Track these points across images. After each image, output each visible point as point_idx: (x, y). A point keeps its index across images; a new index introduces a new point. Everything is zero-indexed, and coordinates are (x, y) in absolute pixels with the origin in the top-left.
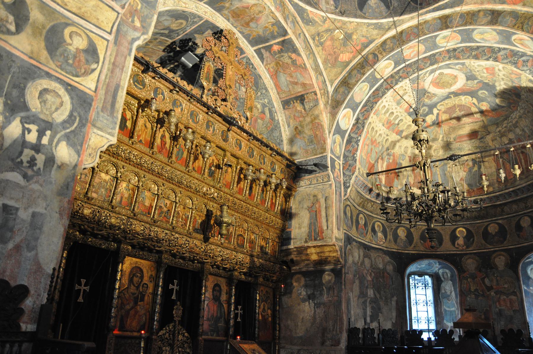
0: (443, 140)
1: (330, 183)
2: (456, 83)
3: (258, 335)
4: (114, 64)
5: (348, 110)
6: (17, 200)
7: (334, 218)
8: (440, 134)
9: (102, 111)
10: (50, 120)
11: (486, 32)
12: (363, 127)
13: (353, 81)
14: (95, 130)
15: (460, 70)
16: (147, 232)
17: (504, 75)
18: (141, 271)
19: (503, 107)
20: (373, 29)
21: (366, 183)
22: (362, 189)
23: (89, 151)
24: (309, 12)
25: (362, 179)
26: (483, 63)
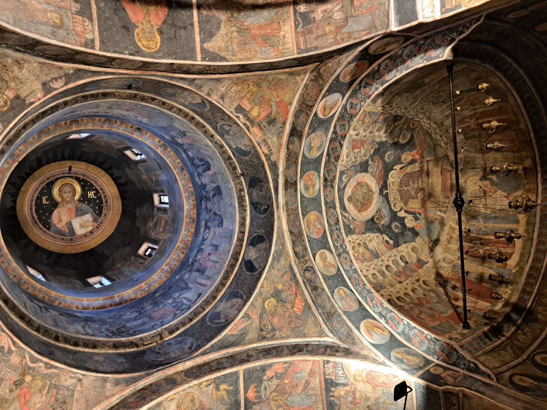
0: (445, 212)
1: (461, 395)
2: (367, 185)
5: (362, 325)
8: (435, 214)
11: (310, 144)
12: (391, 311)
13: (328, 307)
17: (365, 131)
19: (412, 136)
20: (278, 263)
21: (479, 333)
22: (489, 342)
24: (230, 333)
25: (468, 339)
26: (344, 151)
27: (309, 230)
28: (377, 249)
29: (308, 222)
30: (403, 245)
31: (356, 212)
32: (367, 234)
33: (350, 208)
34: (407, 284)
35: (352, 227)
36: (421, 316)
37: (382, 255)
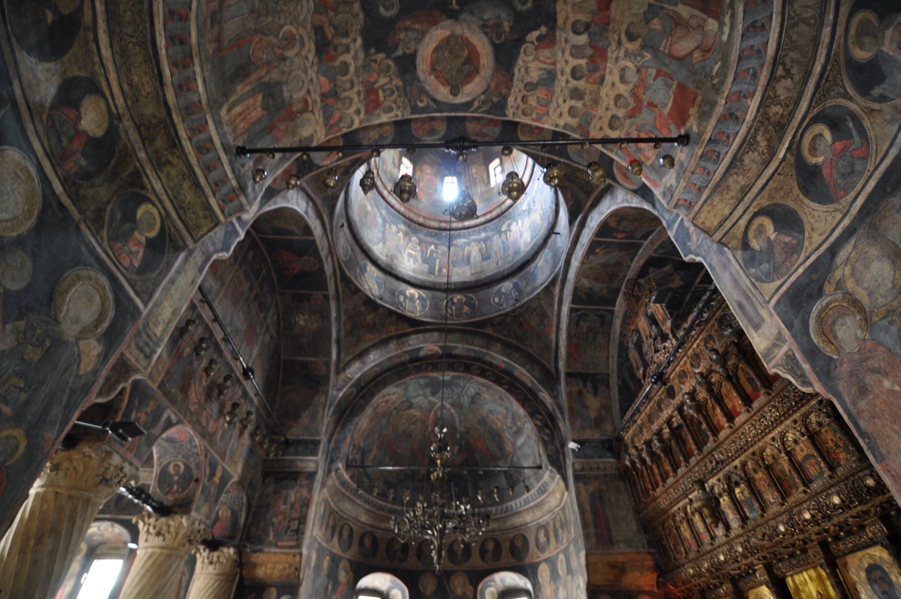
15: (423, 91)
27: (487, 135)
28: (543, 66)
30: (558, 8)
31: (477, 79)
34: (611, 72)
35: (495, 100)
37: (554, 64)
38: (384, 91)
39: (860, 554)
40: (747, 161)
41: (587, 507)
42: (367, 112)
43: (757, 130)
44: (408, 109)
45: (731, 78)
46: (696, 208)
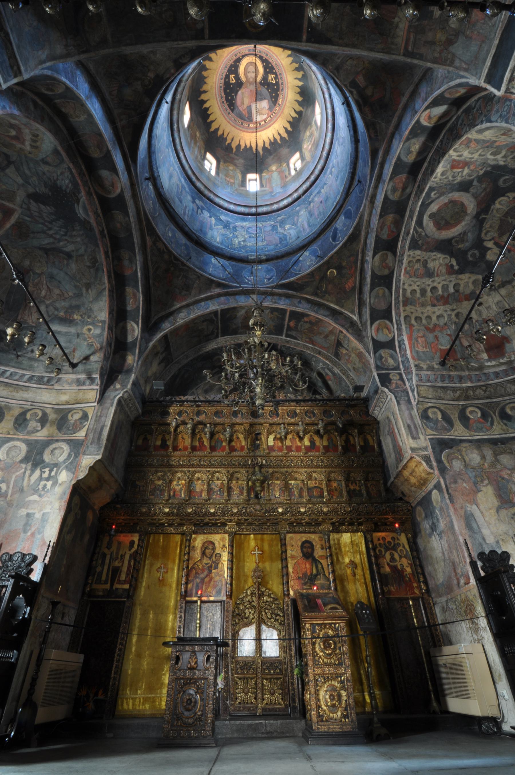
1: (389, 397)
2: (462, 204)
3: (381, 588)
4: (100, 416)
5: (378, 322)
6: (34, 509)
7: (403, 429)
9: (91, 444)
10: (56, 462)
11: (409, 148)
14: (85, 457)
15: (442, 194)
16: (198, 510)
18: (213, 544)
23: (82, 469)
26: (440, 169)
27: (382, 230)
28: (436, 269)
29: (383, 222)
30: (467, 275)
31: (434, 229)
32: (434, 253)
33: (427, 225)
34: (439, 309)
36: (420, 340)
37: (438, 276)
38: (459, 173)
39: (303, 535)
40: (448, 392)
41: (114, 428)
42: (454, 160)
43: (460, 390)
44: (435, 185)
45: (477, 373)
46: (422, 384)
